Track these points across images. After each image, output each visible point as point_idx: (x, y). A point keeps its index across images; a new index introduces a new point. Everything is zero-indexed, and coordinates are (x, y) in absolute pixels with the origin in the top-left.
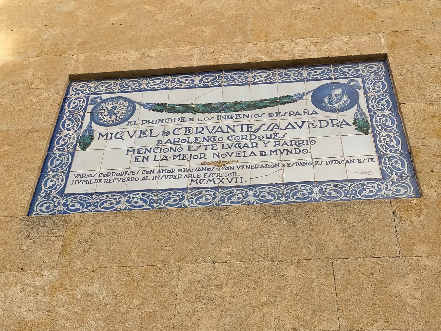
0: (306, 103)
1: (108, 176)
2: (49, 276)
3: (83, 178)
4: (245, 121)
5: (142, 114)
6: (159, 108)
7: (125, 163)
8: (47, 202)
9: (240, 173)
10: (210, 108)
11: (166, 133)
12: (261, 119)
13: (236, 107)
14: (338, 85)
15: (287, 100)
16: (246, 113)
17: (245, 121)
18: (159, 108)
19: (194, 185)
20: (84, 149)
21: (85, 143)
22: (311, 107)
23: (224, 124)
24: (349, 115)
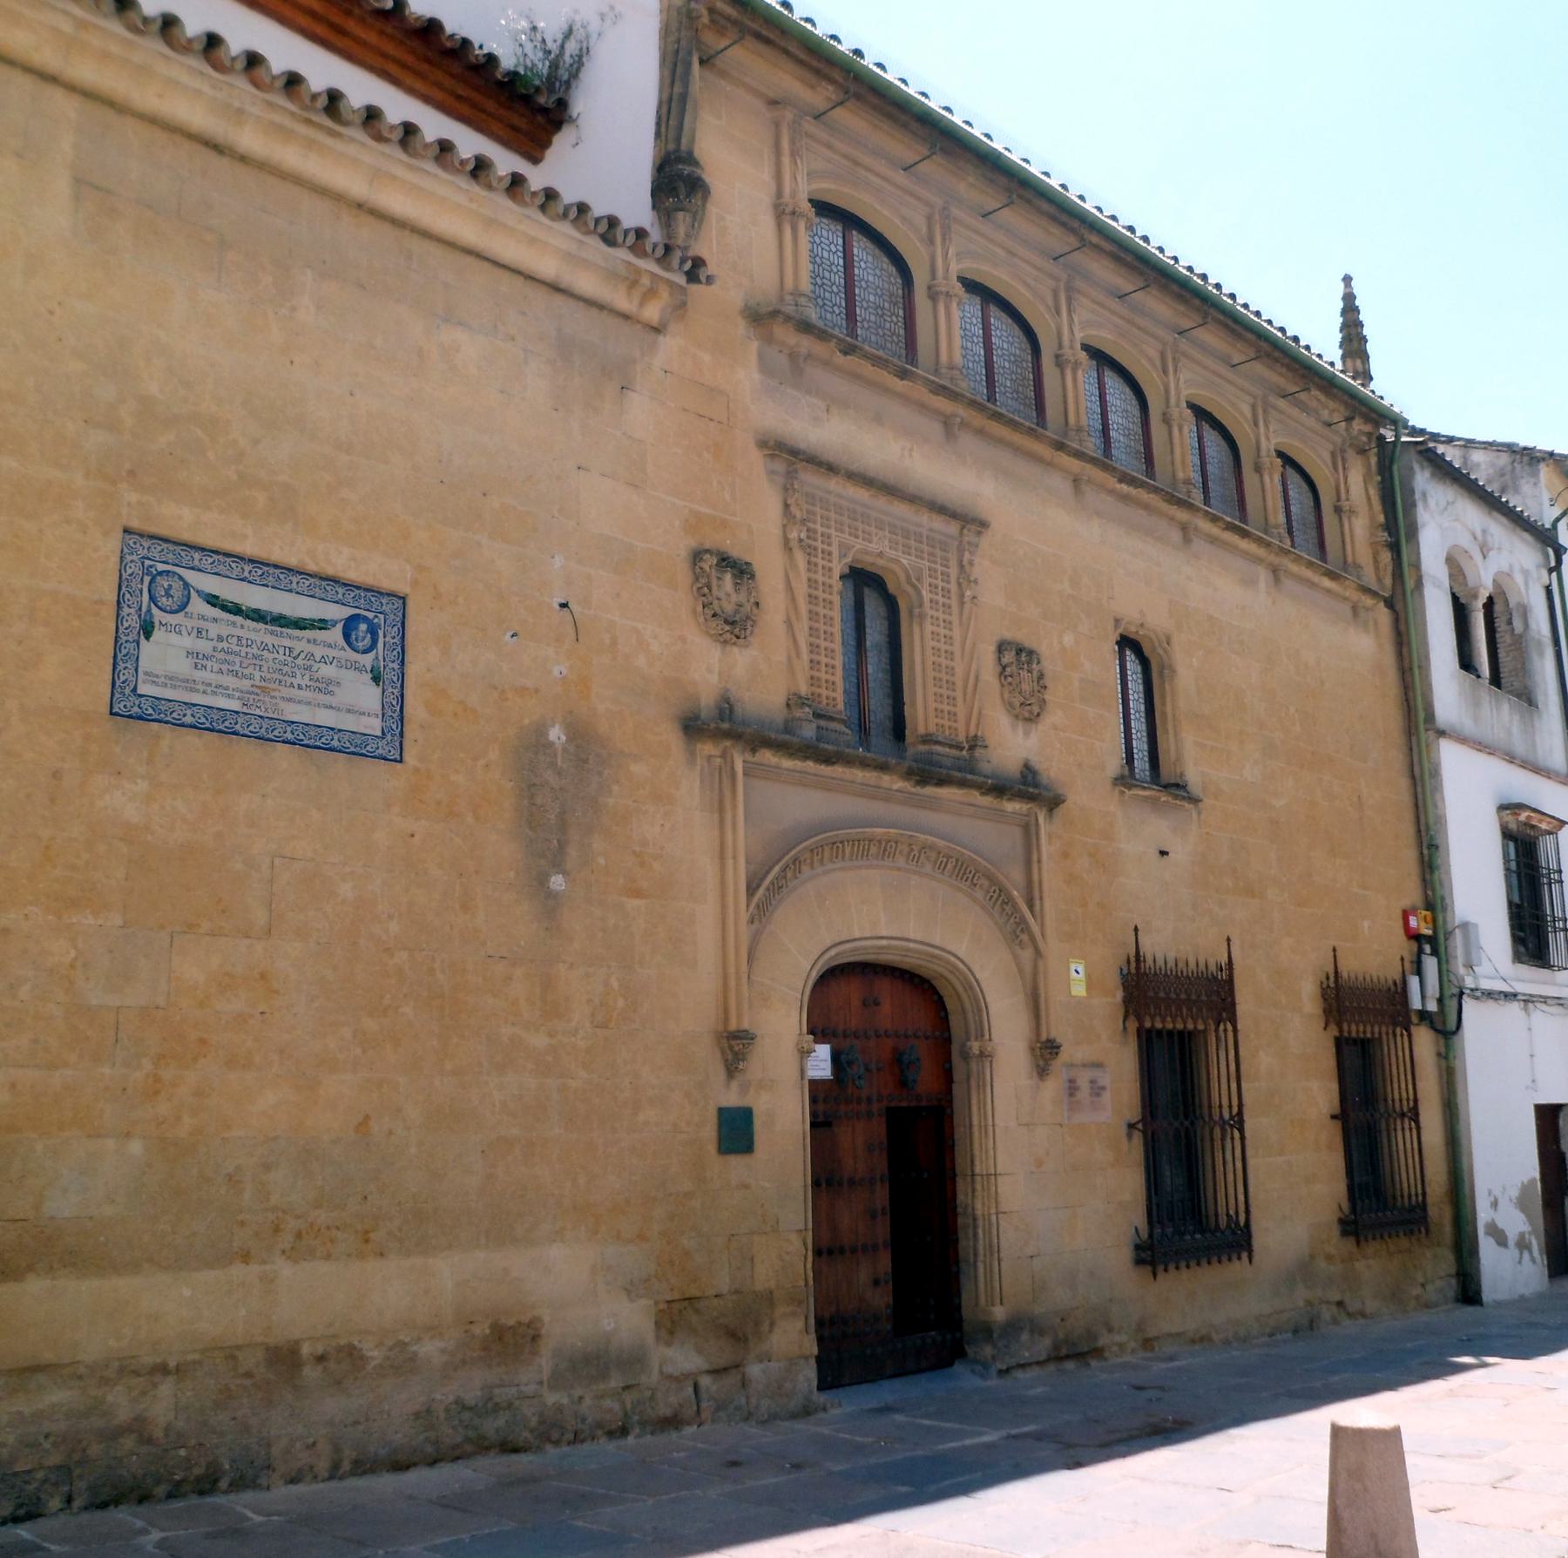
0: (336, 634)
1: (172, 680)
5: (198, 606)
6: (213, 600)
7: (183, 667)
8: (131, 709)
9: (282, 705)
10: (258, 616)
11: (220, 639)
12: (299, 641)
13: (280, 621)
14: (365, 619)
15: (322, 625)
16: (290, 631)
17: (288, 643)
18: (213, 600)
19: (245, 710)
20: (147, 638)
21: (147, 630)
22: (341, 642)
23: (269, 640)
24: (367, 660)
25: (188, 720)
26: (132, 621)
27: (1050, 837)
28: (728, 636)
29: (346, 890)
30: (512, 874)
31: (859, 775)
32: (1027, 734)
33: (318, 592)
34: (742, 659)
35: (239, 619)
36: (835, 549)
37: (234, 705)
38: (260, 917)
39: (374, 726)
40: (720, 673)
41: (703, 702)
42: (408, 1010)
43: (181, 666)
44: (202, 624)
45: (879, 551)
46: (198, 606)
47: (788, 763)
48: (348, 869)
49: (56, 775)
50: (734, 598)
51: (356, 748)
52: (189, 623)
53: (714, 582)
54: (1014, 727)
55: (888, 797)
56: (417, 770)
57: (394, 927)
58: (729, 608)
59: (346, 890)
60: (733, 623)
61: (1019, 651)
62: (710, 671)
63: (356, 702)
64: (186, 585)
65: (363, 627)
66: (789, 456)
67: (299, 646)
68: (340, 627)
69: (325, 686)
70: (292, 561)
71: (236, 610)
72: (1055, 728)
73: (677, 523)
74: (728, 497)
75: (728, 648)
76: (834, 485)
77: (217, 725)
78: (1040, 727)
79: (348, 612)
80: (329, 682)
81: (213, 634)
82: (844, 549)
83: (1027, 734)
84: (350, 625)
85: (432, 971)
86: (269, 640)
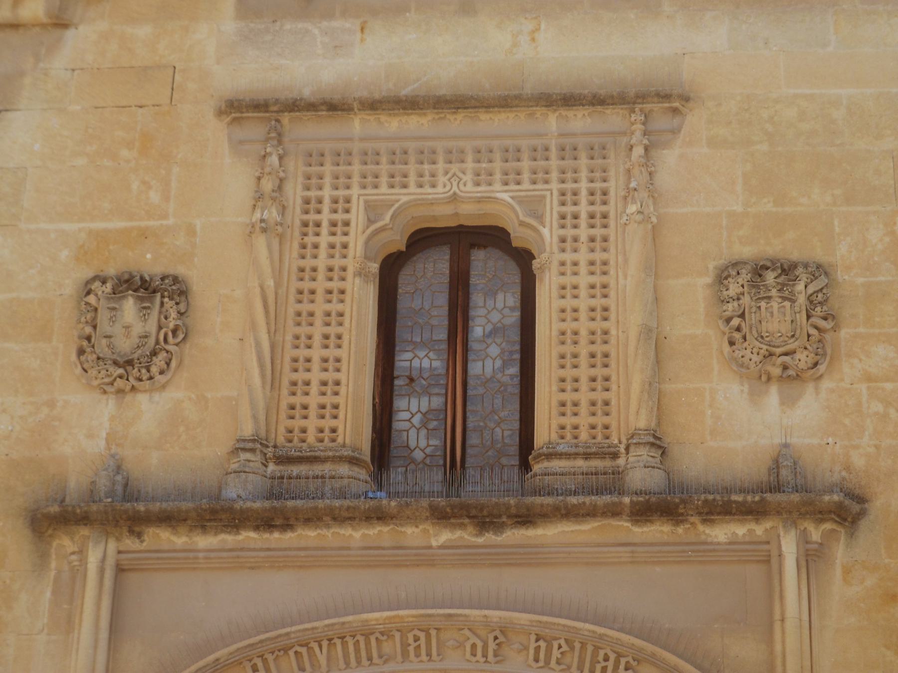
27: (847, 571)
28: (120, 383)
31: (356, 535)
32: (788, 402)
34: (149, 409)
36: (357, 217)
40: (110, 439)
41: (72, 484)
45: (455, 191)
47: (204, 541)
50: (138, 329)
53: (103, 316)
54: (755, 396)
55: (425, 559)
58: (125, 345)
60: (130, 363)
61: (759, 271)
62: (90, 436)
66: (259, 113)
72: (869, 378)
73: (64, 254)
74: (154, 197)
75: (129, 398)
76: (358, 125)
78: (827, 384)
82: (373, 210)
83: (788, 402)
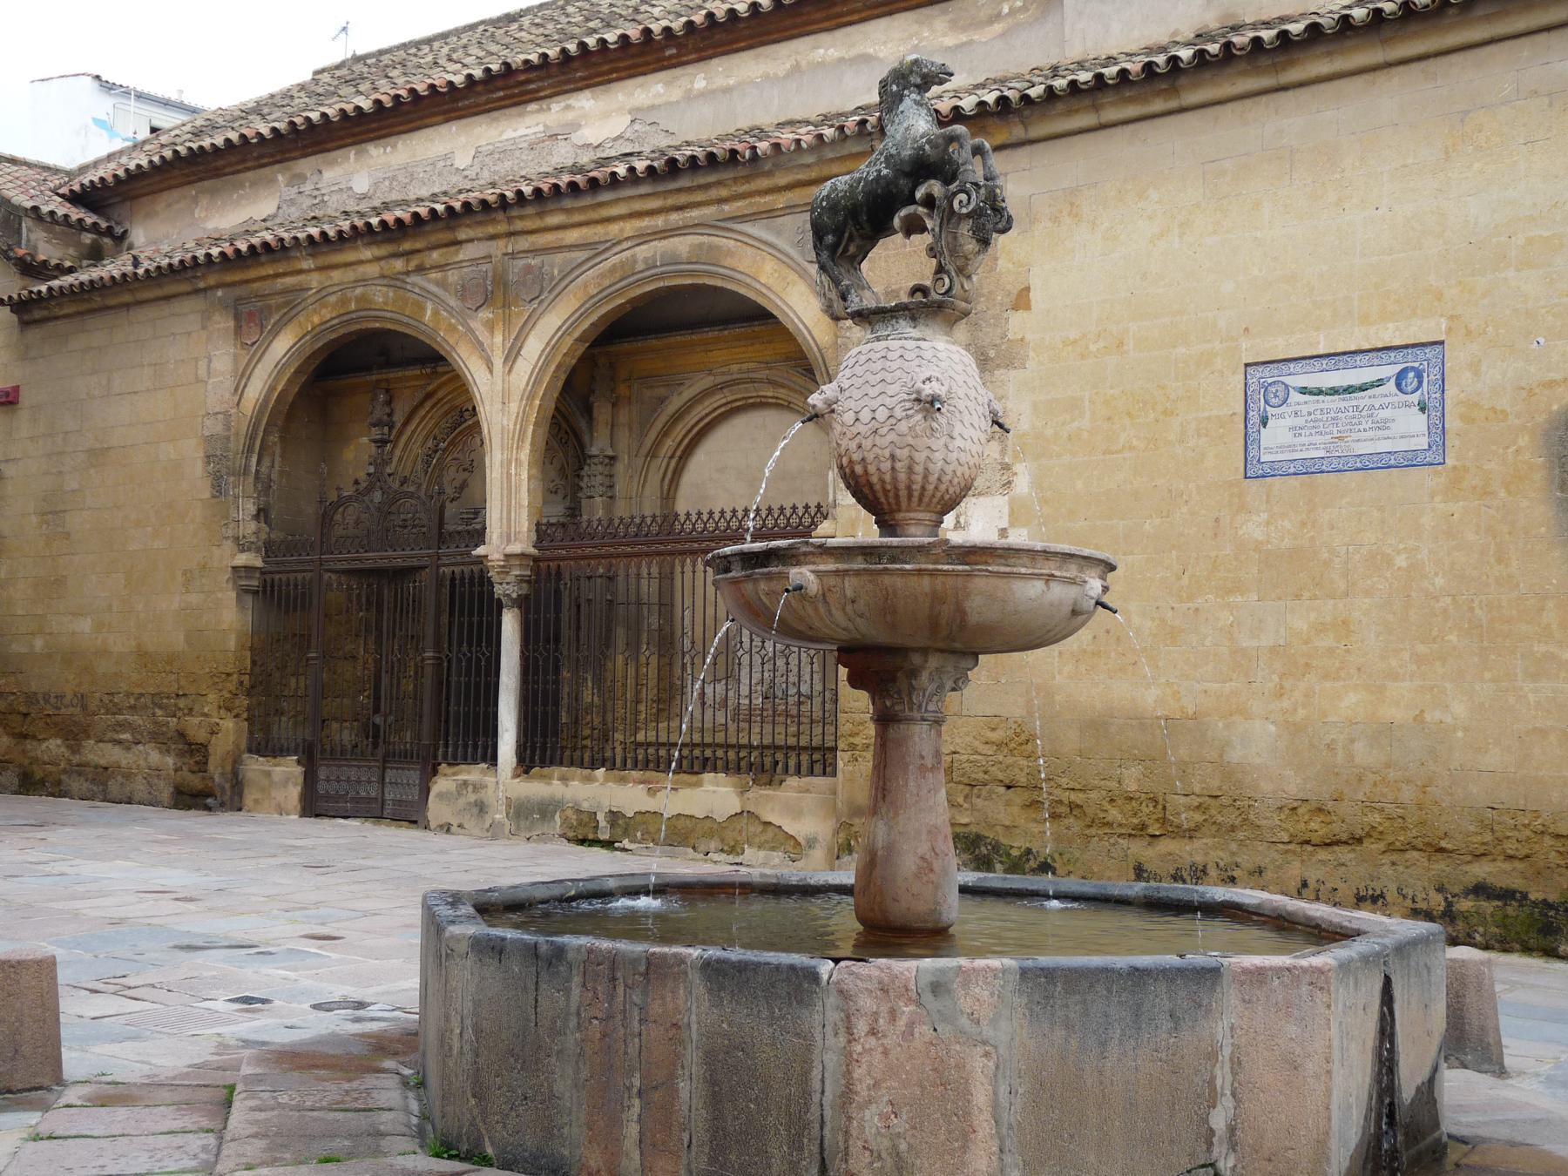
0: (1391, 386)
1: (1282, 448)
2: (1264, 516)
3: (1269, 450)
4: (1354, 403)
5: (1295, 397)
6: (1304, 391)
8: (1254, 470)
9: (1353, 445)
10: (1334, 391)
11: (1309, 414)
12: (1362, 399)
13: (1349, 390)
14: (1413, 368)
15: (1380, 383)
17: (1354, 403)
18: (1304, 391)
21: (1264, 422)
22: (1394, 389)
23: (1342, 405)
24: (1415, 398)
25: (1292, 470)
26: (1254, 418)
29: (1401, 561)
30: (1543, 530)
33: (1376, 362)
35: (1321, 397)
37: (1322, 454)
38: (1342, 585)
39: (1423, 443)
42: (1453, 638)
43: (1286, 438)
44: (1298, 408)
46: (1295, 397)
48: (1401, 546)
49: (1217, 520)
51: (1411, 461)
52: (1290, 410)
56: (1455, 468)
57: (1439, 581)
59: (1401, 561)
63: (1408, 427)
64: (1287, 386)
65: (1411, 375)
67: (1362, 403)
68: (1393, 381)
69: (1383, 425)
70: (1353, 348)
71: (1320, 392)
77: (1309, 469)
79: (1399, 367)
80: (1386, 421)
81: (1305, 412)
84: (1400, 378)
85: (1472, 609)
86: (1342, 405)
